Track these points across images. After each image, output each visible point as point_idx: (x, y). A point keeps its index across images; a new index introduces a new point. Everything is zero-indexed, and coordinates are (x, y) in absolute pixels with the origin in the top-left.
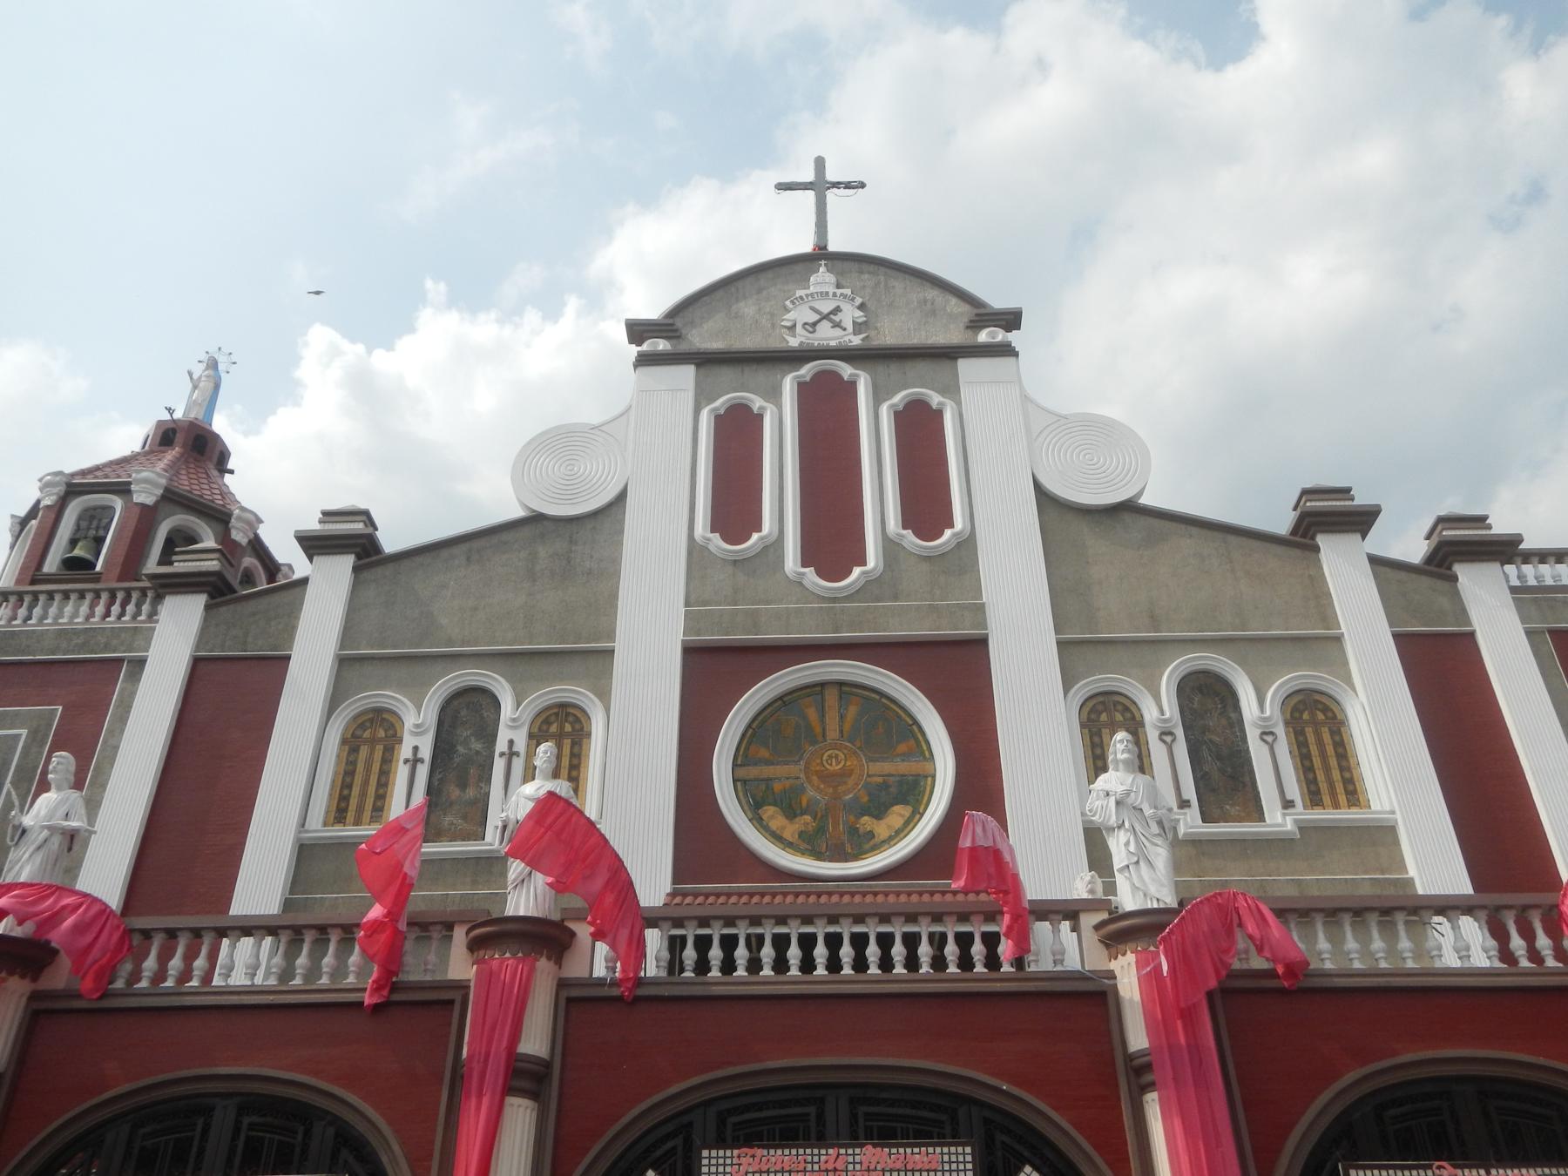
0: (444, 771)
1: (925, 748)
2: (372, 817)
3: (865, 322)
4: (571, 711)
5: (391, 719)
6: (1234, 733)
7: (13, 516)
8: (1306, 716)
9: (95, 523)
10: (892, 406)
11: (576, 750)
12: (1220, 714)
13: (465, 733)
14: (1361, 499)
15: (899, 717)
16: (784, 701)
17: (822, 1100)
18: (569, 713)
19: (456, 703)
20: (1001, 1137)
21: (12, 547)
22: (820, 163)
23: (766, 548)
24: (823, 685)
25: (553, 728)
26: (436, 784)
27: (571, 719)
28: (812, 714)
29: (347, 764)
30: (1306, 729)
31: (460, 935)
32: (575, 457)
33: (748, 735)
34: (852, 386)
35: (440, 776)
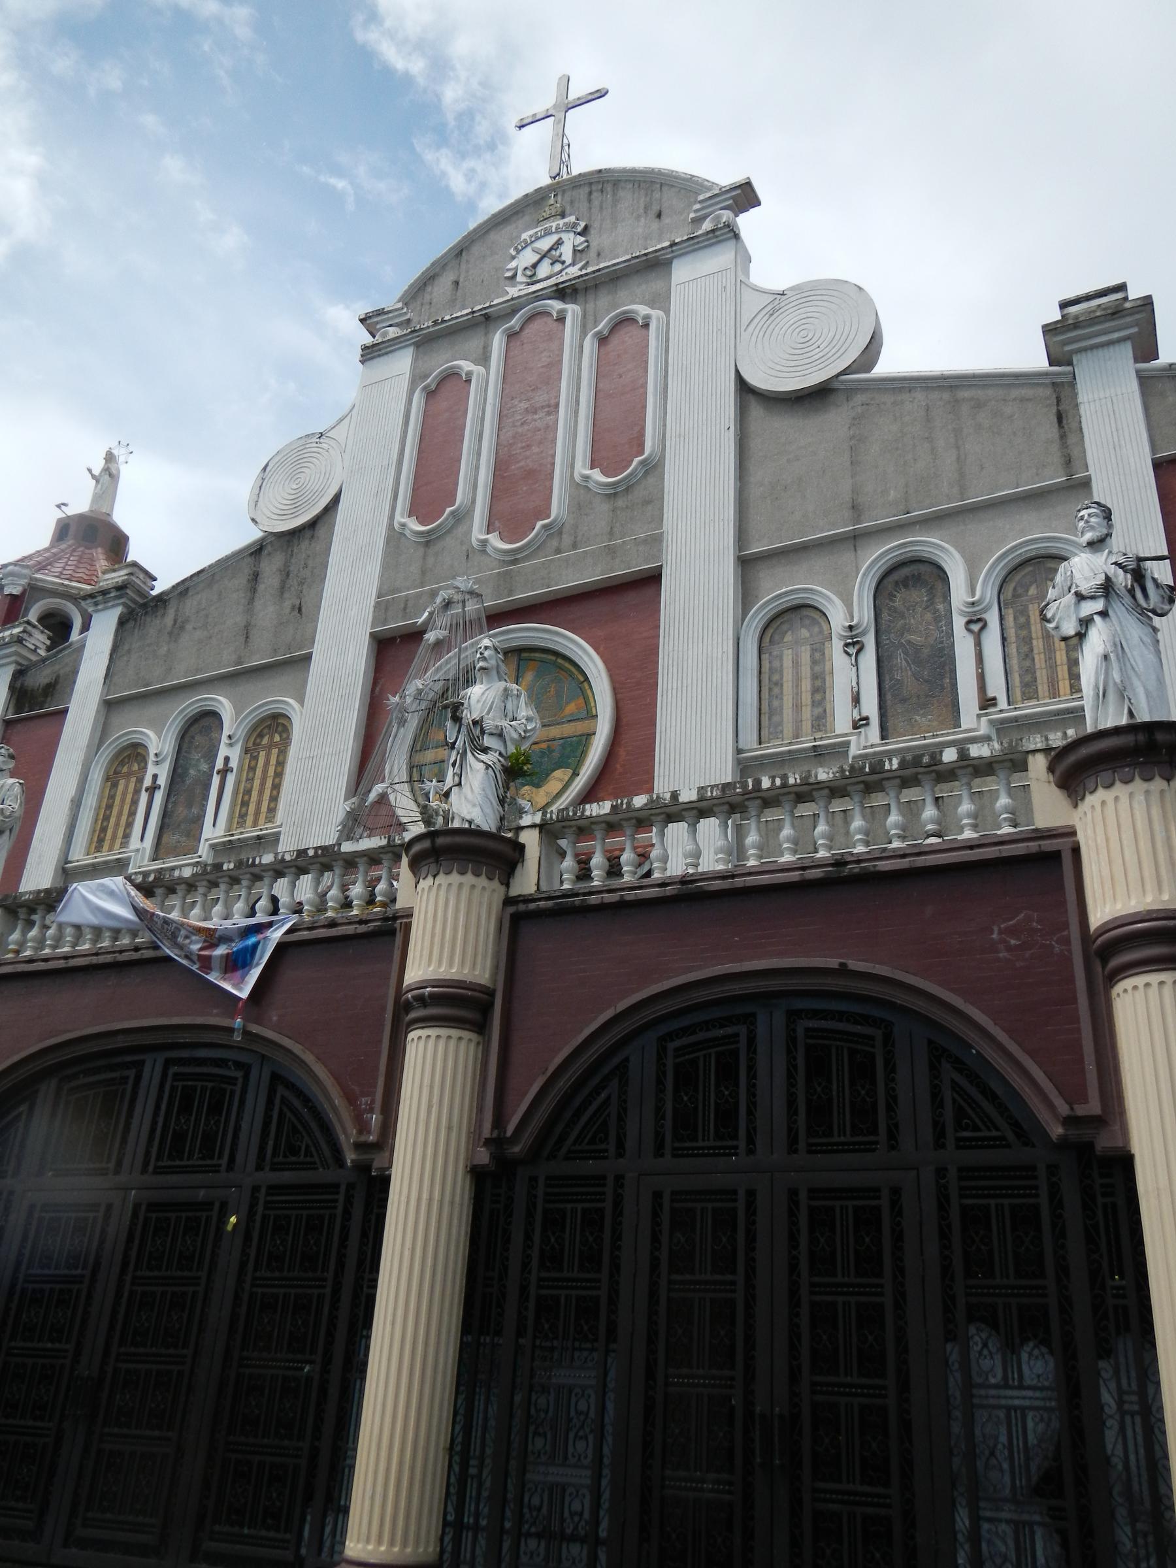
1: (593, 704)
3: (588, 247)
6: (939, 628)
8: (1033, 591)
10: (599, 332)
11: (281, 758)
12: (925, 609)
13: (196, 756)
14: (1134, 293)
15: (571, 675)
17: (143, 1062)
20: (281, 1091)
25: (265, 741)
27: (280, 729)
30: (1031, 606)
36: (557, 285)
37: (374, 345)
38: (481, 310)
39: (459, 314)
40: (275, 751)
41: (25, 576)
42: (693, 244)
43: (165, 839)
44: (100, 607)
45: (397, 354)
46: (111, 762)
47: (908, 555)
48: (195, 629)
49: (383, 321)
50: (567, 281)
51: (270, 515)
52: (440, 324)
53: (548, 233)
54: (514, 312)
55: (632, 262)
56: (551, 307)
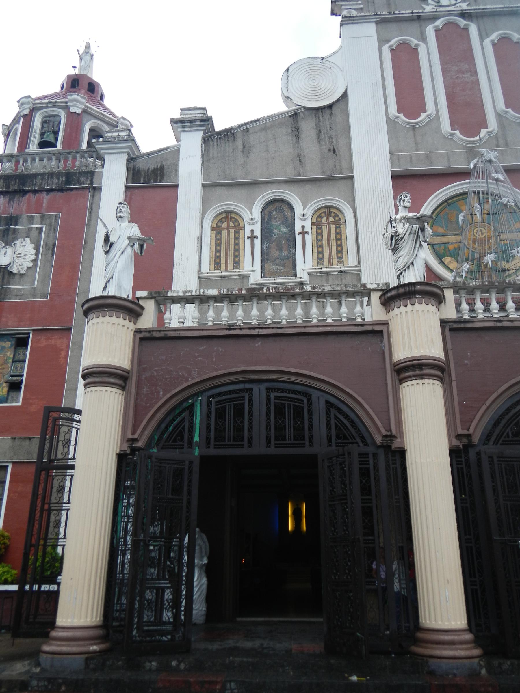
0: (268, 242)
2: (234, 266)
4: (332, 210)
5: (236, 217)
7: (3, 125)
9: (51, 124)
10: (492, 41)
11: (338, 230)
13: (275, 223)
16: (447, 203)
19: (269, 208)
21: (6, 142)
23: (430, 121)
25: (324, 220)
27: (333, 215)
29: (216, 240)
31: (375, 297)
32: (315, 76)
36: (462, 10)
37: (350, 17)
38: (417, 13)
39: (404, 12)
40: (333, 227)
41: (82, 103)
43: (267, 266)
44: (186, 129)
46: (213, 220)
56: (460, 21)
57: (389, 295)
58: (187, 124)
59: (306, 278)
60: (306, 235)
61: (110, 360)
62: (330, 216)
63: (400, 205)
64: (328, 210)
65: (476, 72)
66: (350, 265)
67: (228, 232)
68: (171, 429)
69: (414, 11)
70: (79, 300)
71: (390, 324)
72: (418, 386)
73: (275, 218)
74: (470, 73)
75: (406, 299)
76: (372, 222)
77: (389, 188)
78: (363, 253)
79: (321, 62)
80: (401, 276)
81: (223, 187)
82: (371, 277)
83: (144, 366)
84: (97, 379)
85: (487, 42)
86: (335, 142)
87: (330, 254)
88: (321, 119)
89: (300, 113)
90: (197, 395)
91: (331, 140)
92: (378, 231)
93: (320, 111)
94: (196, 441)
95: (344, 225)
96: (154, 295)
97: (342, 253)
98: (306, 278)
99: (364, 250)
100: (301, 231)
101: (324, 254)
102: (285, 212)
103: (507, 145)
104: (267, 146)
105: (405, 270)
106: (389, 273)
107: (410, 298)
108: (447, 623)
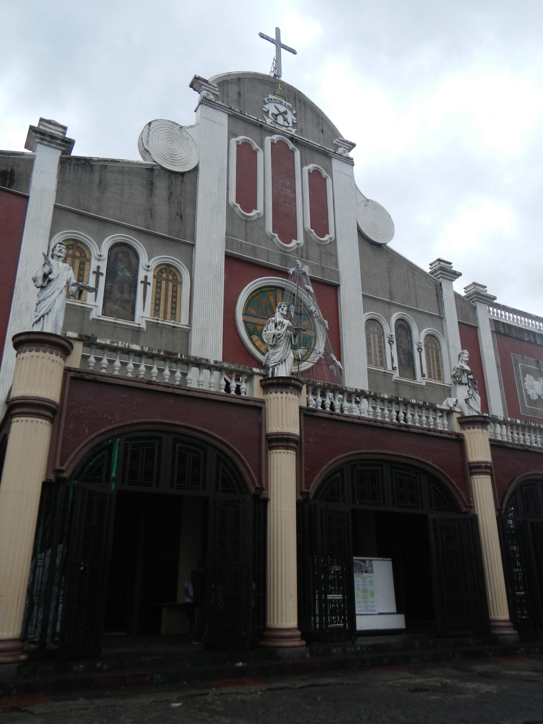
0: (112, 282)
3: (296, 123)
4: (172, 269)
5: (83, 248)
10: (309, 170)
12: (406, 337)
13: (121, 266)
16: (260, 291)
18: (171, 270)
19: (116, 249)
22: (278, 30)
23: (258, 219)
24: (276, 287)
25: (164, 275)
26: (109, 288)
27: (172, 273)
28: (272, 300)
33: (247, 302)
34: (293, 152)
35: (111, 284)
36: (292, 135)
38: (261, 122)
39: (251, 116)
40: (171, 285)
42: (341, 158)
45: (219, 112)
47: (404, 318)
48: (115, 192)
49: (206, 86)
50: (296, 137)
51: (158, 154)
52: (242, 114)
53: (281, 103)
54: (272, 132)
55: (321, 148)
56: (290, 144)
57: (268, 382)
58: (46, 138)
59: (144, 326)
60: (148, 285)
61: (48, 394)
62: (170, 273)
63: (279, 311)
64: (168, 268)
65: (295, 191)
66: (182, 323)
67: (73, 261)
68: (91, 464)
69: (259, 120)
70: (13, 329)
71: (267, 403)
72: (284, 454)
73: (121, 261)
74: (291, 190)
75: (283, 387)
76: (205, 292)
77: (222, 265)
78: (195, 315)
79: (179, 130)
80: (275, 367)
81: (74, 215)
82: (199, 338)
83: (72, 403)
84: (35, 411)
85: (306, 169)
86: (182, 208)
87: (165, 309)
88: (173, 183)
89: (156, 170)
90: (117, 436)
91: (179, 205)
92: (209, 300)
93: (174, 175)
94: (113, 477)
95: (180, 286)
96: (84, 339)
97: (176, 311)
98: (144, 326)
99: (196, 314)
100: (143, 280)
101: (161, 307)
102: (130, 258)
103: (308, 258)
104: (123, 190)
105: (279, 364)
106: (214, 339)
107: (285, 388)
108: (289, 624)
